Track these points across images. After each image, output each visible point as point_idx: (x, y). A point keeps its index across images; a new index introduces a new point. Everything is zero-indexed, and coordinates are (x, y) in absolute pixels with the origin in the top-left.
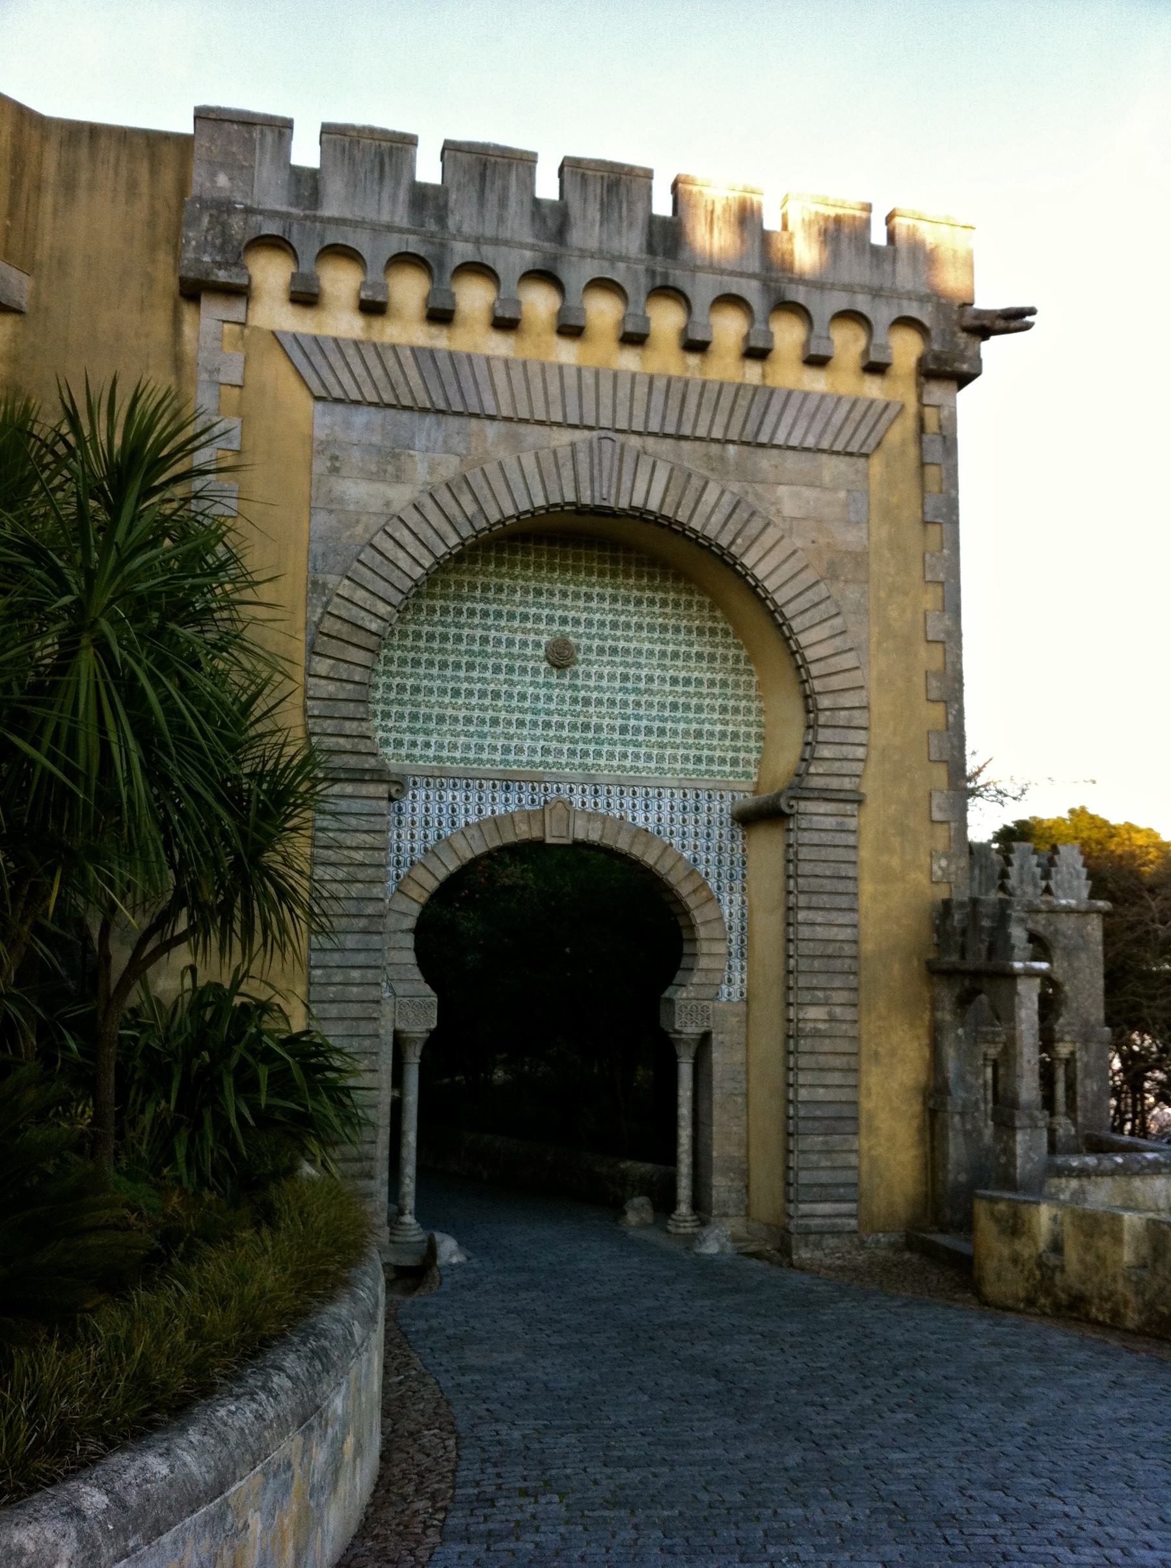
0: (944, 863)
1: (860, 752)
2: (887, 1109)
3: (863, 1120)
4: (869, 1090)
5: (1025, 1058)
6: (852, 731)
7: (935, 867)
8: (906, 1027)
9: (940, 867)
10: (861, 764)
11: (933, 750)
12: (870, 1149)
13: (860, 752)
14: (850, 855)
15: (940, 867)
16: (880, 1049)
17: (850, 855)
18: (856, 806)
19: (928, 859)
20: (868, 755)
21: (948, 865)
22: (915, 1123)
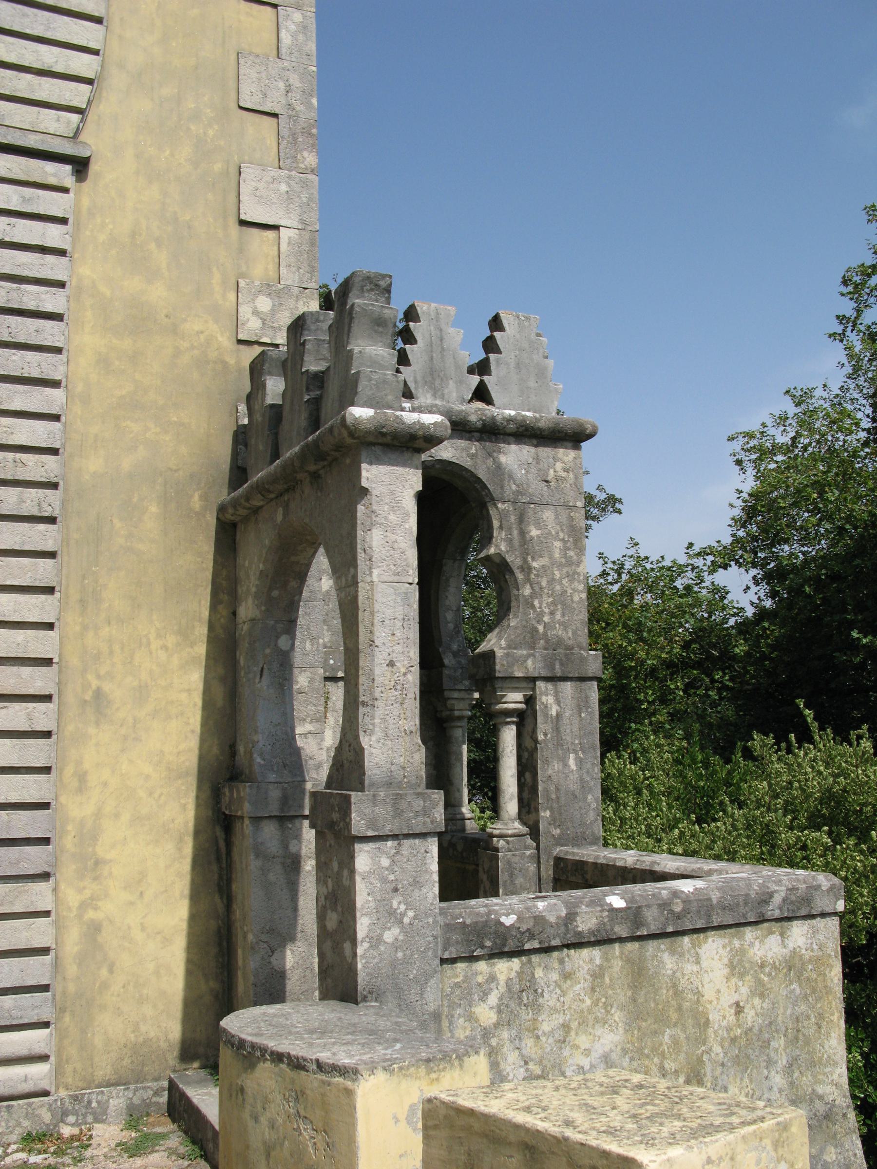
0: (264, 304)
1: (82, 64)
2: (126, 817)
3: (68, 842)
4: (82, 778)
5: (381, 657)
6: (66, 19)
7: (245, 311)
8: (171, 640)
9: (256, 313)
10: (85, 88)
11: (245, 89)
12: (83, 906)
13: (82, 64)
14: (50, 266)
15: (256, 313)
16: (107, 687)
17: (50, 266)
18: (68, 168)
19: (232, 296)
20: (101, 74)
21: (273, 311)
22: (188, 849)
